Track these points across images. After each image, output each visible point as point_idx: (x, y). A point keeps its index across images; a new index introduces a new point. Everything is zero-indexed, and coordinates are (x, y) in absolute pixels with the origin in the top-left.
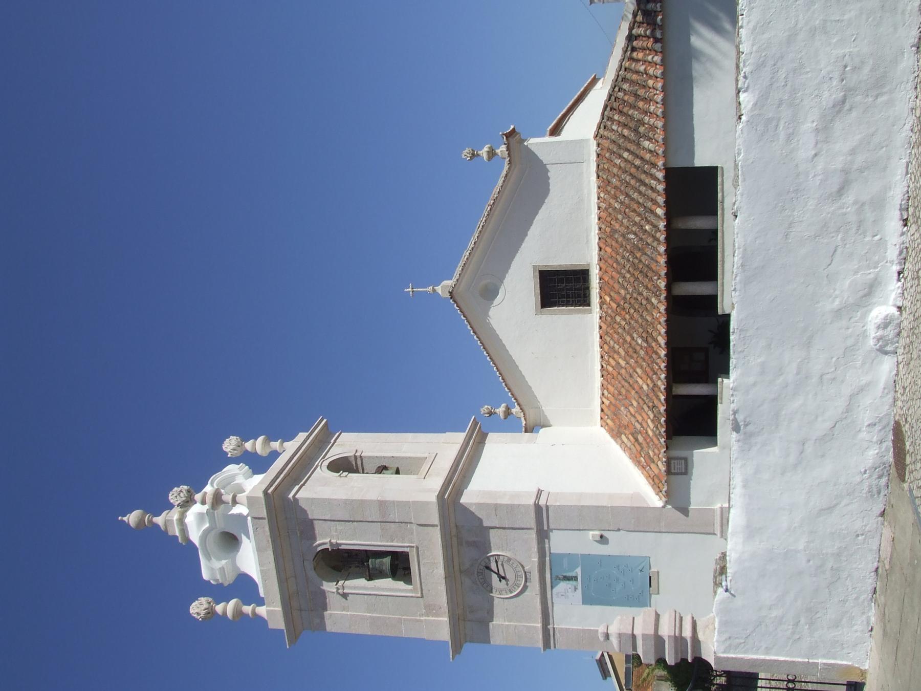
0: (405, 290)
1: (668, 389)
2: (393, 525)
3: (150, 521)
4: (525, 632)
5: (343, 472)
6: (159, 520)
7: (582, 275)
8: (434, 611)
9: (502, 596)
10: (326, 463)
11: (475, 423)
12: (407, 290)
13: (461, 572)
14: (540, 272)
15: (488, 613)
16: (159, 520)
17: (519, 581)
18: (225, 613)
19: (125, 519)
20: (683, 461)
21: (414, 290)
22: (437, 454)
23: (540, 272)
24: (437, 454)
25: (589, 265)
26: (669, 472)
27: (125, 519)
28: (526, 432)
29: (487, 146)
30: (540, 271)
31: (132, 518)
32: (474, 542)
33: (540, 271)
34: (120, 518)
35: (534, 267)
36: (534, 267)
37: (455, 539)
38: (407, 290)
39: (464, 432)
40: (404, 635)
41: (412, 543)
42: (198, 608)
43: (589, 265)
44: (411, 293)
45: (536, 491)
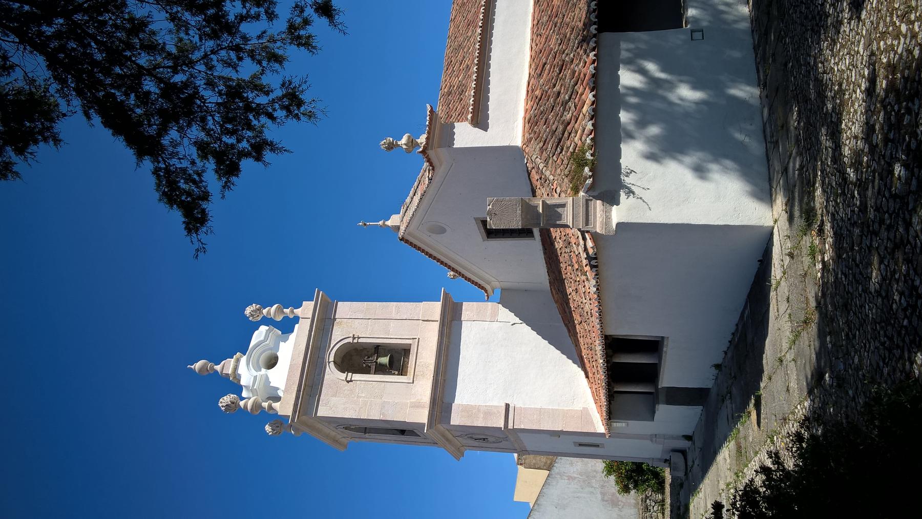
3: (212, 368)
5: (348, 372)
6: (218, 368)
10: (332, 359)
11: (446, 294)
19: (193, 367)
27: (193, 367)
31: (198, 366)
34: (188, 366)
45: (504, 405)
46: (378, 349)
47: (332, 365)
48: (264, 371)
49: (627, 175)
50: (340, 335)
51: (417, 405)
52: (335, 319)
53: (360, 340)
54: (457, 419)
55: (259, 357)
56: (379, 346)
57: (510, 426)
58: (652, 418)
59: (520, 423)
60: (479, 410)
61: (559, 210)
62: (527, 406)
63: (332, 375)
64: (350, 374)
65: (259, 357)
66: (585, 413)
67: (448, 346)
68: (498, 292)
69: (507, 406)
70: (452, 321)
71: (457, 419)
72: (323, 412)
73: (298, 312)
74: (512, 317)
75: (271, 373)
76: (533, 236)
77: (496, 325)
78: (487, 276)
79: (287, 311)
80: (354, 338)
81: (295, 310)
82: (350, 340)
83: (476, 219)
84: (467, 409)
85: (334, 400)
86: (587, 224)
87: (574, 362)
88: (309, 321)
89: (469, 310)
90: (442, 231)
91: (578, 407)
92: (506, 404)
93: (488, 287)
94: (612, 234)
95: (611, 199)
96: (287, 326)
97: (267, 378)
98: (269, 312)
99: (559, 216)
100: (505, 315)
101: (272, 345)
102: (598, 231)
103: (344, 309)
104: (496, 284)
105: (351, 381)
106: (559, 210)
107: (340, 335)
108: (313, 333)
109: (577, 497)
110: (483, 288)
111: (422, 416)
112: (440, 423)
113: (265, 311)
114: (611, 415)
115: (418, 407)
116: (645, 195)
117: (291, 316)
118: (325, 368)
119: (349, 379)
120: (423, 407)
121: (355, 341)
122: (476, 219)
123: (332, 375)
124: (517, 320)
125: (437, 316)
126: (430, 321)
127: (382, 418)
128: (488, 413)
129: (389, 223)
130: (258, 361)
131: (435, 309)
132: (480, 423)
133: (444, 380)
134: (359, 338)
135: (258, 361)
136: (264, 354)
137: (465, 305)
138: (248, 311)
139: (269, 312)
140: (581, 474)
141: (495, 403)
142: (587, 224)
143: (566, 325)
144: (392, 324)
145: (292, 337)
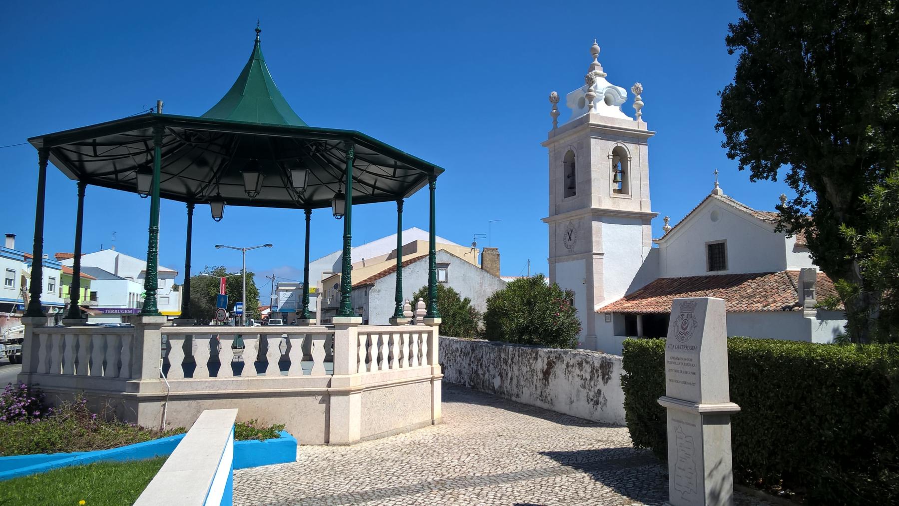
1: (639, 314)
7: (723, 267)
10: (619, 145)
11: (655, 215)
13: (570, 220)
14: (724, 243)
19: (595, 43)
22: (324, 273)
23: (724, 243)
24: (324, 273)
25: (728, 269)
26: (607, 313)
27: (595, 43)
37: (579, 217)
39: (651, 211)
43: (728, 269)
45: (603, 252)
46: (624, 173)
47: (616, 145)
48: (604, 97)
49: (826, 323)
50: (631, 148)
51: (600, 202)
52: (639, 145)
53: (629, 162)
54: (595, 224)
55: (613, 95)
56: (624, 174)
57: (594, 256)
58: (616, 335)
59: (596, 260)
60: (600, 238)
61: (811, 297)
62: (604, 266)
63: (611, 145)
64: (612, 157)
65: (613, 95)
66: (602, 299)
67: (629, 217)
68: (657, 246)
69: (602, 254)
70: (641, 219)
71: (595, 224)
72: (593, 141)
73: (640, 120)
74: (645, 256)
75: (603, 101)
76: (710, 271)
77: (641, 246)
78: (671, 241)
79: (640, 112)
80: (630, 158)
81: (640, 117)
82: (629, 156)
83: (726, 240)
84: (599, 230)
85: (598, 148)
86: (807, 307)
87: (626, 292)
88: (637, 129)
89: (647, 228)
90: (714, 218)
91: (605, 295)
92: (604, 254)
93: (663, 241)
94: (804, 317)
95: (818, 317)
96: (627, 109)
97: (600, 100)
98: (638, 100)
99: (808, 296)
100: (646, 251)
101: (618, 101)
102: (805, 312)
103: (644, 149)
104: (664, 246)
105: (609, 158)
106: (811, 297)
107: (631, 148)
108: (633, 132)
109: (471, 289)
110: (663, 238)
111: (595, 205)
112: (593, 215)
113: (639, 97)
114: (605, 314)
115: (599, 201)
116: (820, 329)
117: (636, 115)
118: (614, 141)
119: (610, 157)
120: (599, 205)
121: (629, 159)
122: (726, 240)
123: (611, 145)
124: (644, 259)
125: (643, 211)
126: (641, 205)
127: (592, 179)
128: (599, 243)
129: (718, 188)
130: (609, 93)
131: (647, 210)
132: (594, 239)
133: (613, 216)
134: (630, 161)
135: (609, 93)
136: (612, 96)
137: (651, 226)
138: (639, 85)
139: (638, 100)
140: (484, 291)
141: (604, 247)
142: (807, 307)
143: (646, 288)
144: (638, 182)
145: (623, 116)
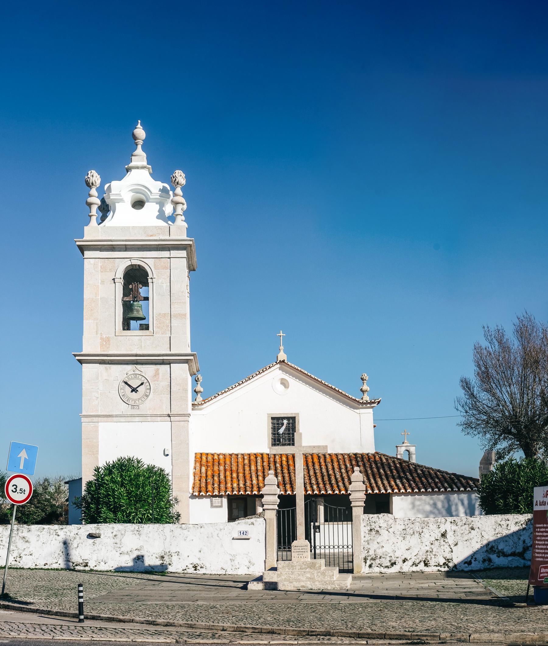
0: (281, 331)
2: (168, 321)
4: (93, 404)
6: (139, 151)
8: (105, 343)
9: (119, 389)
12: (281, 332)
15: (106, 379)
16: (139, 151)
17: (132, 402)
18: (90, 196)
19: (139, 126)
20: (220, 505)
21: (281, 337)
27: (139, 126)
28: (192, 404)
29: (368, 388)
30: (295, 417)
31: (140, 132)
32: (158, 374)
33: (295, 417)
35: (298, 414)
36: (298, 414)
38: (281, 332)
40: (85, 321)
41: (156, 334)
42: (95, 177)
44: (279, 335)
